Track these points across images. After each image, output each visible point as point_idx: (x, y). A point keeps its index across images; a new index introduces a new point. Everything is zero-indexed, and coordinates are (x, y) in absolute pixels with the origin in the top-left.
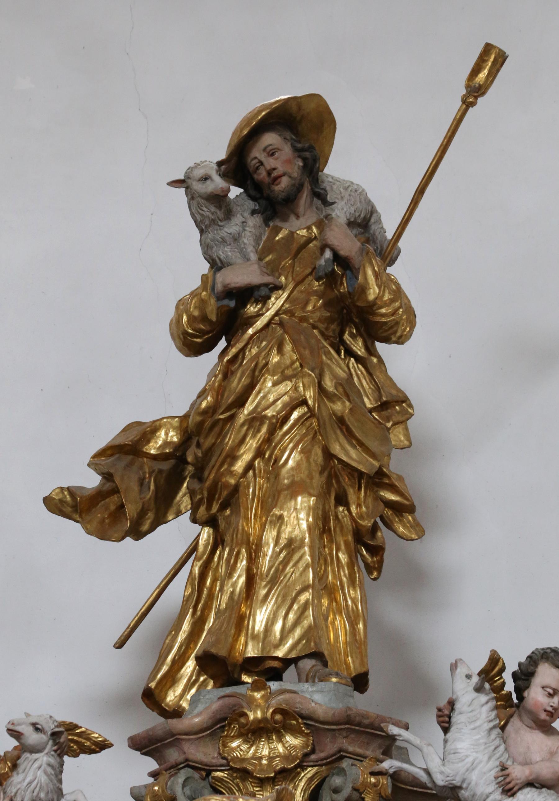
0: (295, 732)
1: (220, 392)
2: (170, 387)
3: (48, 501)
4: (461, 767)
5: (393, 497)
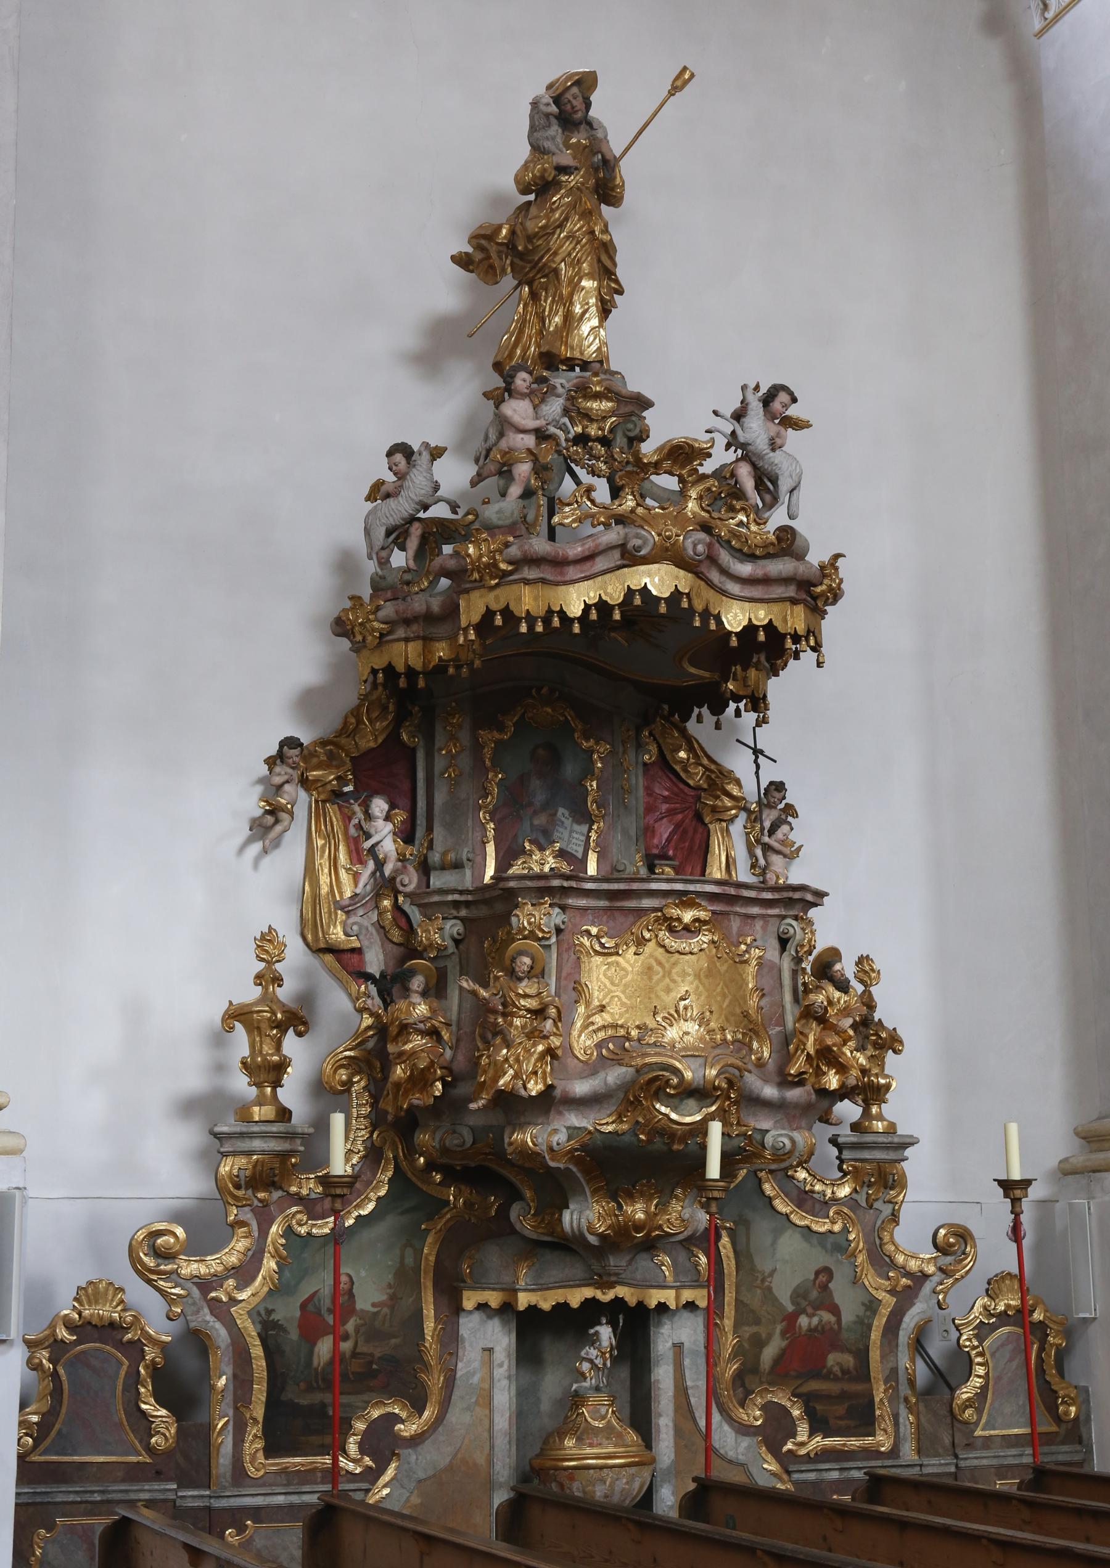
0: (609, 399)
3: (453, 258)
4: (754, 435)
5: (613, 285)
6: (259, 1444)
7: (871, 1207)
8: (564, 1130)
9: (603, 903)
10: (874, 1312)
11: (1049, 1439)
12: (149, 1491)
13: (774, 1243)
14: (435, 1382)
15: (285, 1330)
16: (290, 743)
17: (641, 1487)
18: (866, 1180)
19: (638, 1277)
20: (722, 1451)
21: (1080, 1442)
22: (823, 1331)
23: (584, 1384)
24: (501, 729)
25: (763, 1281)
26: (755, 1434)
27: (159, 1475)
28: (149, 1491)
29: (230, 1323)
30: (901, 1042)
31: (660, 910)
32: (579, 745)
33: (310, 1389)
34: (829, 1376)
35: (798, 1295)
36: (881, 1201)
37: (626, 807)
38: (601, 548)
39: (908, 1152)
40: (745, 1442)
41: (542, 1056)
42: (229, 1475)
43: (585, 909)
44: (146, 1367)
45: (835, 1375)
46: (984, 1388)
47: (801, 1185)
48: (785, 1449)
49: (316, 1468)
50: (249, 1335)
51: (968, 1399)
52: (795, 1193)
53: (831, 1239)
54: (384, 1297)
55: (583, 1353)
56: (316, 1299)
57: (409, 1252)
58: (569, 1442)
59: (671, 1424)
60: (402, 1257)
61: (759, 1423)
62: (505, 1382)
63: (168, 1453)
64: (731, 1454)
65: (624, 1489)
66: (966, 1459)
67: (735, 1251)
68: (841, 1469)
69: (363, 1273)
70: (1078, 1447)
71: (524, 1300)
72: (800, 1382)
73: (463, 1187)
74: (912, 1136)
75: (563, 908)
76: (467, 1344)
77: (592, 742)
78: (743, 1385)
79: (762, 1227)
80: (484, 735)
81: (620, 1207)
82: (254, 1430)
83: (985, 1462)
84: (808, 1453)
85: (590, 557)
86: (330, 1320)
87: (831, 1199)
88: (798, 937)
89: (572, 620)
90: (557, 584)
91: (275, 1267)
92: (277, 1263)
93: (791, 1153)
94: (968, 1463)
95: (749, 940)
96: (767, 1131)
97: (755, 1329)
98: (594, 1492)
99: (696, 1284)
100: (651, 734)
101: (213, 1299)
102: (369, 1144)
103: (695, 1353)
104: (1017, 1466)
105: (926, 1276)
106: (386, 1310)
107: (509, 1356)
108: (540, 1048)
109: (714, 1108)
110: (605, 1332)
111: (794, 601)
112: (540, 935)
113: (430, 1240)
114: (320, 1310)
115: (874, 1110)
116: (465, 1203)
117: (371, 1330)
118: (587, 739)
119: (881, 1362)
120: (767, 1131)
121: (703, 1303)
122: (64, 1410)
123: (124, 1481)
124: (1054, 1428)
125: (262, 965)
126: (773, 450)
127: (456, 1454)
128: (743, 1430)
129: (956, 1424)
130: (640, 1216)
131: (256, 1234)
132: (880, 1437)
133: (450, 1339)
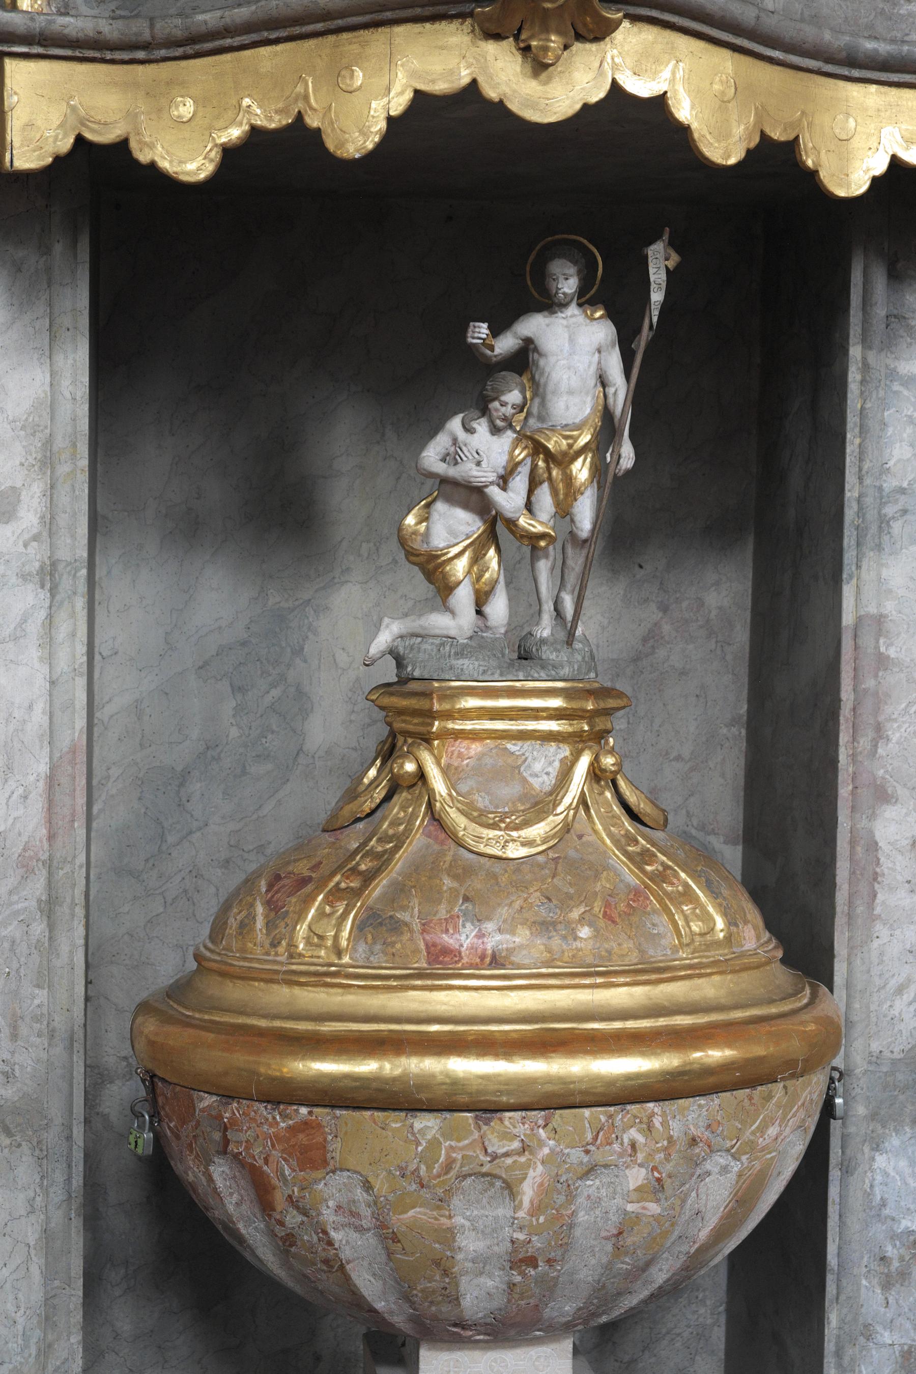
17: (743, 1201)
23: (439, 622)
55: (432, 456)
98: (448, 1236)
107: (47, 461)
110: (578, 354)
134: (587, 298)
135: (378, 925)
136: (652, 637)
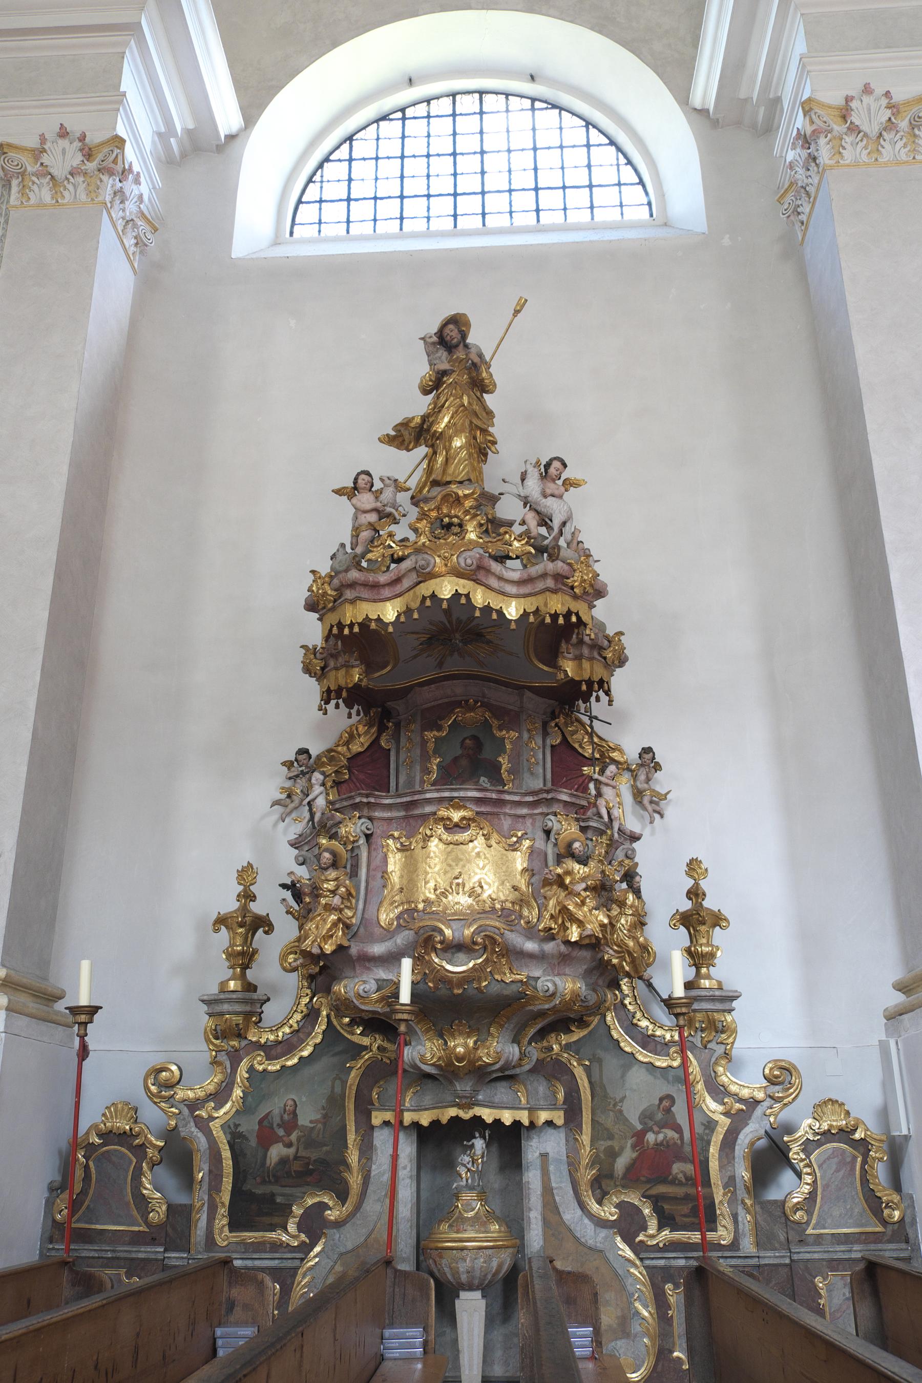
1: (435, 404)
2: (420, 405)
6: (225, 1221)
7: (706, 1048)
8: (373, 982)
9: (402, 813)
10: (713, 1130)
11: (875, 1238)
12: (145, 1252)
13: (623, 1076)
14: (354, 1180)
15: (247, 1139)
16: (304, 751)
17: (500, 1266)
18: (697, 1025)
19: (497, 1100)
20: (583, 1240)
21: (907, 1242)
22: (668, 1146)
24: (439, 728)
25: (615, 1105)
26: (611, 1227)
27: (153, 1241)
28: (145, 1252)
29: (208, 1133)
30: (726, 920)
31: (435, 813)
32: (493, 735)
33: (264, 1182)
34: (674, 1182)
35: (646, 1116)
36: (714, 1042)
37: (532, 774)
38: (402, 572)
39: (735, 1004)
40: (603, 1233)
41: (335, 925)
42: (203, 1242)
43: (390, 819)
44: (148, 1163)
45: (680, 1181)
46: (812, 1195)
47: (644, 1031)
48: (638, 1239)
49: (265, 1241)
50: (221, 1142)
51: (798, 1203)
52: (640, 1036)
53: (672, 1073)
54: (319, 1116)
56: (269, 1117)
57: (338, 1082)
58: (444, 1227)
59: (540, 1217)
60: (333, 1087)
61: (615, 1218)
62: (408, 1181)
63: (161, 1226)
64: (591, 1242)
65: (482, 1267)
66: (799, 1253)
67: (590, 1082)
68: (686, 1258)
69: (304, 1099)
70: (904, 1246)
71: (408, 1118)
72: (648, 1186)
73: (377, 1036)
74: (736, 991)
75: (370, 819)
76: (379, 1152)
77: (504, 732)
78: (600, 1187)
79: (611, 1063)
80: (429, 735)
81: (446, 1043)
82: (223, 1211)
83: (816, 1256)
84: (658, 1243)
85: (398, 580)
86: (281, 1132)
87: (669, 1042)
88: (555, 828)
89: (388, 624)
90: (375, 601)
91: (241, 1095)
92: (243, 1091)
93: (553, 995)
94: (801, 1256)
95: (520, 834)
96: (539, 978)
97: (609, 1143)
99: (553, 1107)
100: (557, 725)
101: (197, 1116)
102: (310, 1006)
103: (558, 1161)
104: (846, 1260)
105: (758, 1102)
106: (320, 1125)
108: (333, 917)
109: (481, 960)
110: (479, 1144)
111: (554, 591)
112: (352, 839)
113: (353, 1074)
114: (272, 1124)
115: (704, 970)
116: (378, 1048)
117: (309, 1141)
118: (501, 730)
119: (720, 1170)
120: (539, 978)
121: (560, 1121)
122: (91, 1192)
123: (129, 1244)
124: (880, 1229)
125: (242, 888)
126: (545, 497)
127: (370, 1235)
128: (601, 1223)
129: (789, 1223)
130: (460, 1050)
131: (229, 1071)
132: (721, 1232)
133: (367, 1149)
134: (480, 1137)
135: (450, 1226)
136: (508, 1185)
